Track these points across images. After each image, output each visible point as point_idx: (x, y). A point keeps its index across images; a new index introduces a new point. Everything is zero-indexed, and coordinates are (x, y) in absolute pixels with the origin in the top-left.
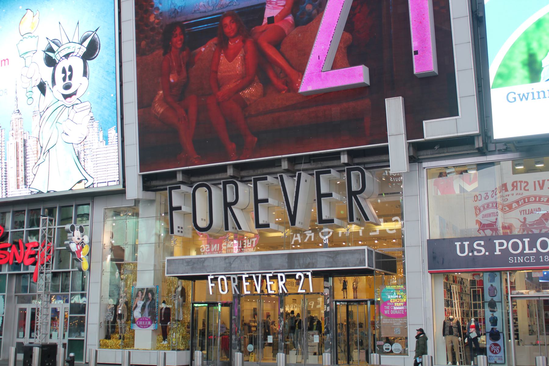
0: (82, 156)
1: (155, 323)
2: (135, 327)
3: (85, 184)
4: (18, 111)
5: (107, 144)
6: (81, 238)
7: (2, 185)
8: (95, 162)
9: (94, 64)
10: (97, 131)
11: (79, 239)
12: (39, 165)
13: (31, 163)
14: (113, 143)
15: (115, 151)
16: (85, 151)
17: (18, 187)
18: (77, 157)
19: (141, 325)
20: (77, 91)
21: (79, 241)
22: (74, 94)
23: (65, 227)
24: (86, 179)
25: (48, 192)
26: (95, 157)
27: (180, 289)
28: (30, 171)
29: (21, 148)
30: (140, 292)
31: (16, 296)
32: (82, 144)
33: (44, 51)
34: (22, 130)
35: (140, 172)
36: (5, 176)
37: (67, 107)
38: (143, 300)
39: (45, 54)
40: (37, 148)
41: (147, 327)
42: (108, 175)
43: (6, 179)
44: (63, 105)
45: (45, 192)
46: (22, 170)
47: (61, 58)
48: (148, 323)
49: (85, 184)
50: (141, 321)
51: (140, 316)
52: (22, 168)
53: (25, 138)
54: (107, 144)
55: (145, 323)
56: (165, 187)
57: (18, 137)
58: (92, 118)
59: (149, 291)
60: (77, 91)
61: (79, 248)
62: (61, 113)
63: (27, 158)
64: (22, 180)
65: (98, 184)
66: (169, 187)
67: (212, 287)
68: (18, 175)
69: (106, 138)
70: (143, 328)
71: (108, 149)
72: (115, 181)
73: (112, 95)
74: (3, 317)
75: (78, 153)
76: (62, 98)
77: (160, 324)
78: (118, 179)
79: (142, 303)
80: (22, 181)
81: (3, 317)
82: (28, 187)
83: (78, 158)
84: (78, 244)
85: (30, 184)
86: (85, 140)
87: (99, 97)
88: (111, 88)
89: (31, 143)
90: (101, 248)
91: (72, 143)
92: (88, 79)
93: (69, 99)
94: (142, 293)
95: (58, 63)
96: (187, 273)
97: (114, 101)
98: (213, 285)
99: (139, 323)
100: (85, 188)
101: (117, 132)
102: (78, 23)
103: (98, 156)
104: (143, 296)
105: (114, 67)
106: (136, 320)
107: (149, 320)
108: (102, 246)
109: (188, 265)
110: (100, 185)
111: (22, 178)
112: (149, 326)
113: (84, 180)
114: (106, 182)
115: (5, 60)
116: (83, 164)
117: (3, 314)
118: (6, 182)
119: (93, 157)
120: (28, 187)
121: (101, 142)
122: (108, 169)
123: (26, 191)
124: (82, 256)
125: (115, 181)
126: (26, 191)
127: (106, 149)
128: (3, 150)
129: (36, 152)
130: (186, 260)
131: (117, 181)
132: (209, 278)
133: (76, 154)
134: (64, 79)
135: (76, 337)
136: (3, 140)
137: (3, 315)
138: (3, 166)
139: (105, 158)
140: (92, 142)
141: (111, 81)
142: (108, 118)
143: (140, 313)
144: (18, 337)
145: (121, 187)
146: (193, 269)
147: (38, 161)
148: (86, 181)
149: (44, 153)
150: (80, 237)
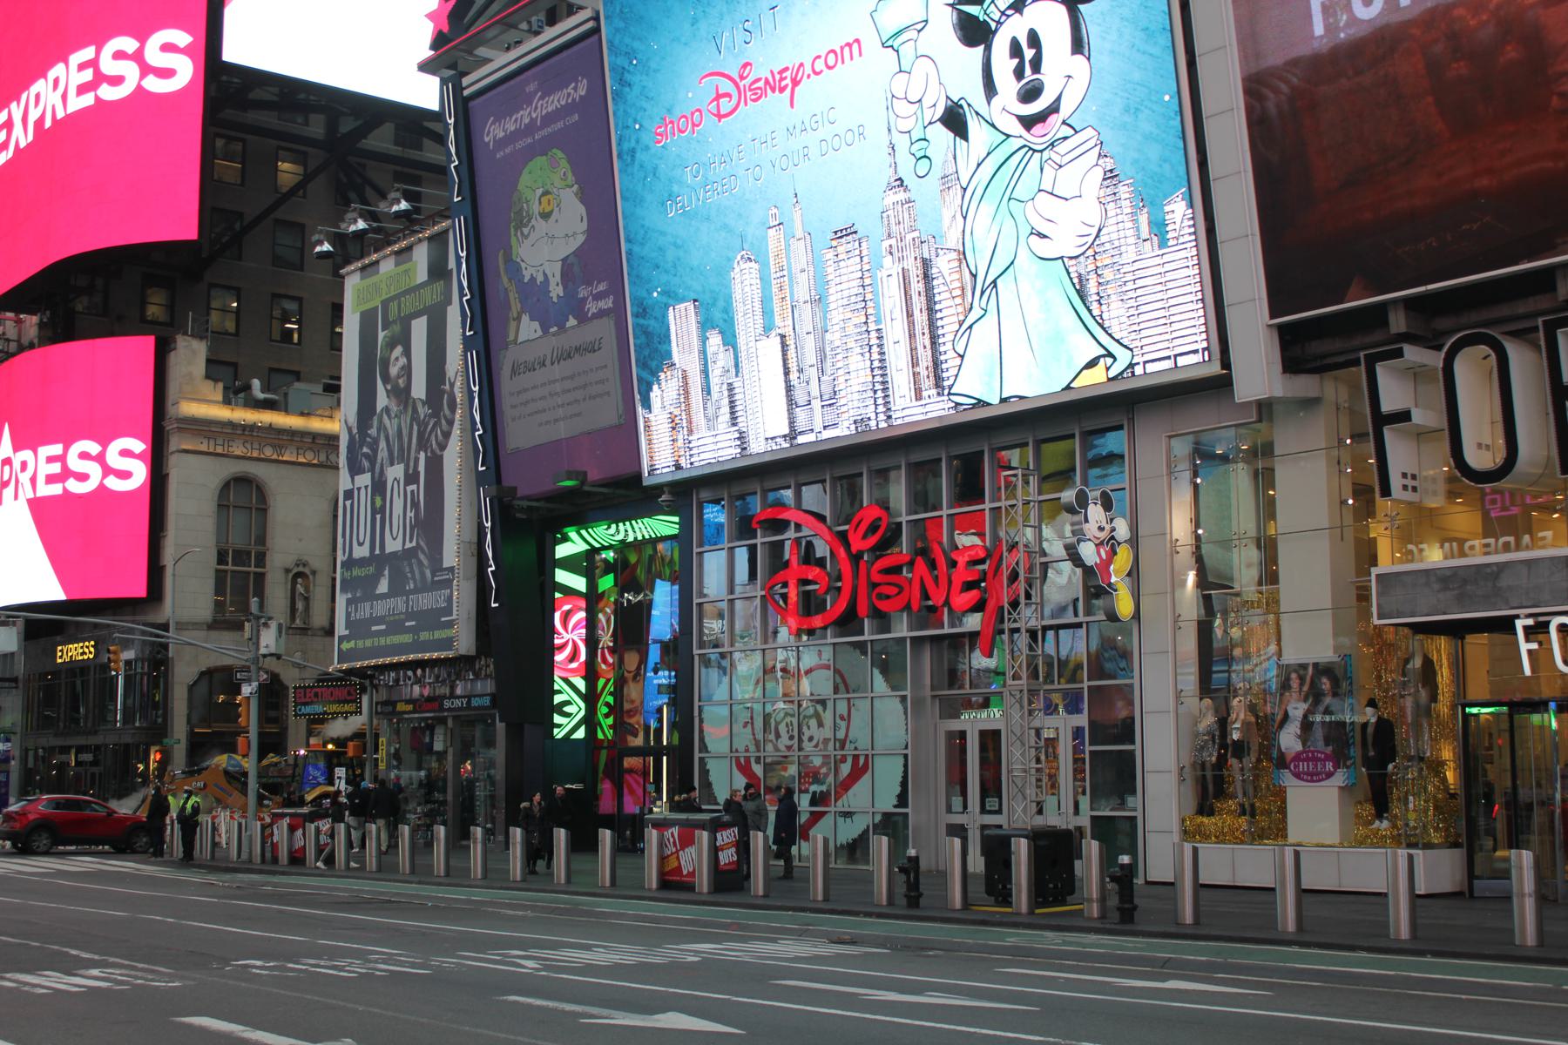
0: (1092, 287)
1: (1348, 767)
2: (1287, 779)
3: (1108, 369)
4: (898, 183)
5: (1163, 244)
6: (1108, 527)
7: (875, 392)
8: (1132, 303)
9: (1102, 14)
10: (1129, 211)
11: (1101, 529)
12: (970, 327)
13: (948, 324)
14: (1180, 241)
15: (1190, 264)
16: (1099, 273)
17: (918, 397)
18: (1078, 291)
19: (1308, 774)
20: (1059, 98)
21: (1102, 535)
22: (1054, 108)
23: (1060, 498)
24: (1110, 355)
25: (1003, 400)
26: (1130, 286)
27: (1417, 662)
28: (949, 346)
29: (917, 286)
30: (1294, 676)
31: (934, 697)
32: (1090, 252)
34: (916, 234)
35: (1272, 316)
36: (881, 368)
37: (1035, 151)
38: (1305, 700)
39: (955, 13)
40: (961, 279)
41: (1320, 780)
42: (1175, 335)
43: (882, 375)
44: (1025, 146)
45: (996, 401)
46: (925, 347)
47: (1003, 13)
48: (1325, 766)
49: (1108, 369)
50: (1303, 760)
51: (1299, 747)
53: (926, 255)
54: (1163, 244)
55: (1316, 765)
56: (1351, 356)
57: (905, 254)
58: (1110, 176)
59: (1322, 670)
60: (1059, 98)
61: (1104, 556)
62: (1021, 169)
63: (936, 312)
65: (1147, 365)
66: (1544, 321)
67: (1530, 652)
69: (1159, 229)
70: (1312, 781)
71: (1167, 258)
72: (1196, 352)
73: (1167, 98)
74: (906, 756)
75: (1080, 281)
76: (1017, 128)
77: (1364, 770)
78: (1205, 344)
79: (1303, 707)
80: (928, 377)
81: (906, 756)
82: (946, 392)
83: (1082, 294)
84: (1102, 543)
86: (1097, 242)
87: (1127, 110)
88: (1162, 76)
89: (944, 265)
90: (1168, 551)
91: (1062, 258)
92: (1089, 59)
93: (1038, 129)
94: (1302, 679)
95: (997, 30)
96: (1445, 614)
97: (1172, 115)
98: (1534, 646)
99: (1295, 767)
100: (1110, 380)
101: (1191, 205)
103: (1140, 283)
104: (1305, 688)
105: (1163, 12)
106: (1288, 758)
107: (1327, 758)
108: (1168, 545)
109: (1445, 589)
110: (1151, 368)
111: (927, 368)
112: (1329, 775)
113: (1104, 356)
114: (1169, 358)
115: (849, 45)
116: (1096, 313)
117: (906, 747)
118: (883, 383)
120: (946, 392)
121: (1145, 241)
122: (1173, 319)
123: (941, 405)
124: (1113, 579)
125: (1196, 352)
126: (941, 405)
128: (869, 297)
129: (958, 292)
130: (1438, 572)
131: (1204, 349)
132: (1519, 624)
133: (1074, 284)
134: (1019, 73)
135: (1111, 810)
136: (866, 267)
137: (905, 752)
138: (874, 341)
139: (1159, 288)
140: (1117, 243)
141: (1158, 58)
142: (1161, 166)
143: (1299, 737)
144: (949, 810)
145: (1215, 369)
146: (1463, 601)
148: (1109, 361)
149: (983, 293)
150: (1104, 524)
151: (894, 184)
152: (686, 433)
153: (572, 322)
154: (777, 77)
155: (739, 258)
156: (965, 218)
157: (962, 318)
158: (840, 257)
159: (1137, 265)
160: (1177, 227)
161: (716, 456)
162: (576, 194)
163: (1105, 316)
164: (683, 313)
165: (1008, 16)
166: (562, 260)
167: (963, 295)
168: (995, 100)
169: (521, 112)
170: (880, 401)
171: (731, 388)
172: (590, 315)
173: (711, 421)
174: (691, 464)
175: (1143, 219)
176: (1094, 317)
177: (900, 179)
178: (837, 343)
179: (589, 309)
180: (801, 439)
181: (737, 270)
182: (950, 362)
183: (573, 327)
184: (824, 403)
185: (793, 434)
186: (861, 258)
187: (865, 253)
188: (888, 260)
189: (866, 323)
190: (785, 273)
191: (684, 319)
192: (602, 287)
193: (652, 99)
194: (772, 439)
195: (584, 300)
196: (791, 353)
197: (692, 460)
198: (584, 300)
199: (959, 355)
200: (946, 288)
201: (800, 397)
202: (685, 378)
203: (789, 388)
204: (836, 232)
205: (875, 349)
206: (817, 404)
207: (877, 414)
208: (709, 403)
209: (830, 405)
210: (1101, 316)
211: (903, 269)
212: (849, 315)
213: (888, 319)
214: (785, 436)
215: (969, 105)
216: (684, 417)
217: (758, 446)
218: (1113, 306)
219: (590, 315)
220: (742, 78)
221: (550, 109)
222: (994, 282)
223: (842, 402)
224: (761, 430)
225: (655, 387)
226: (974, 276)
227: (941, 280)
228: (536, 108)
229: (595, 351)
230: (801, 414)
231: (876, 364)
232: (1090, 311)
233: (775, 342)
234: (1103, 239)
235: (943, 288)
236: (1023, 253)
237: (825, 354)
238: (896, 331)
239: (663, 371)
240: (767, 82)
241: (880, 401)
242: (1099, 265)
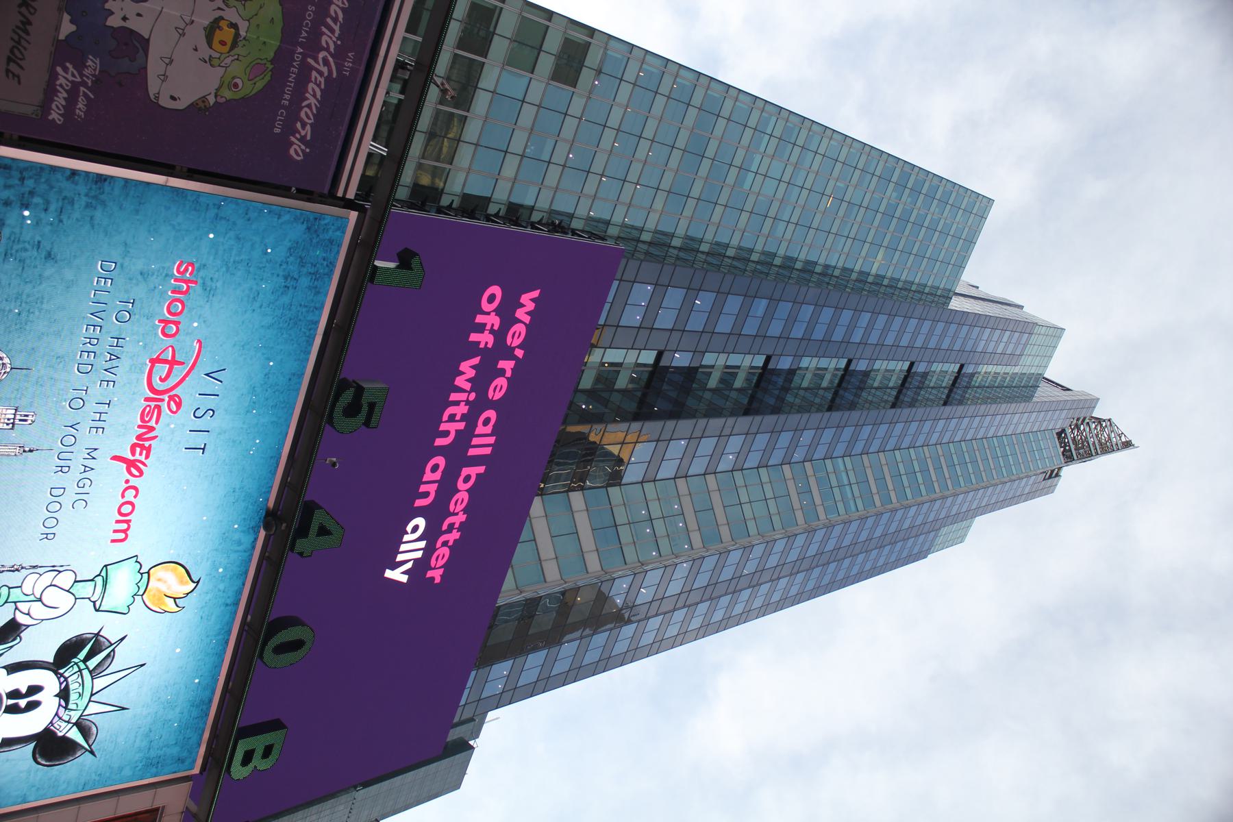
33: (98, 634)
102: (123, 709)
153: (67, 28)
162: (204, 99)
165: (61, 684)
166: (148, 41)
169: (337, 32)
172: (59, 69)
179: (66, 70)
183: (58, 29)
192: (81, 105)
195: (80, 66)
198: (80, 66)
215: (11, 647)
219: (59, 69)
220: (171, 398)
221: (311, 86)
228: (326, 62)
229: (9, 60)
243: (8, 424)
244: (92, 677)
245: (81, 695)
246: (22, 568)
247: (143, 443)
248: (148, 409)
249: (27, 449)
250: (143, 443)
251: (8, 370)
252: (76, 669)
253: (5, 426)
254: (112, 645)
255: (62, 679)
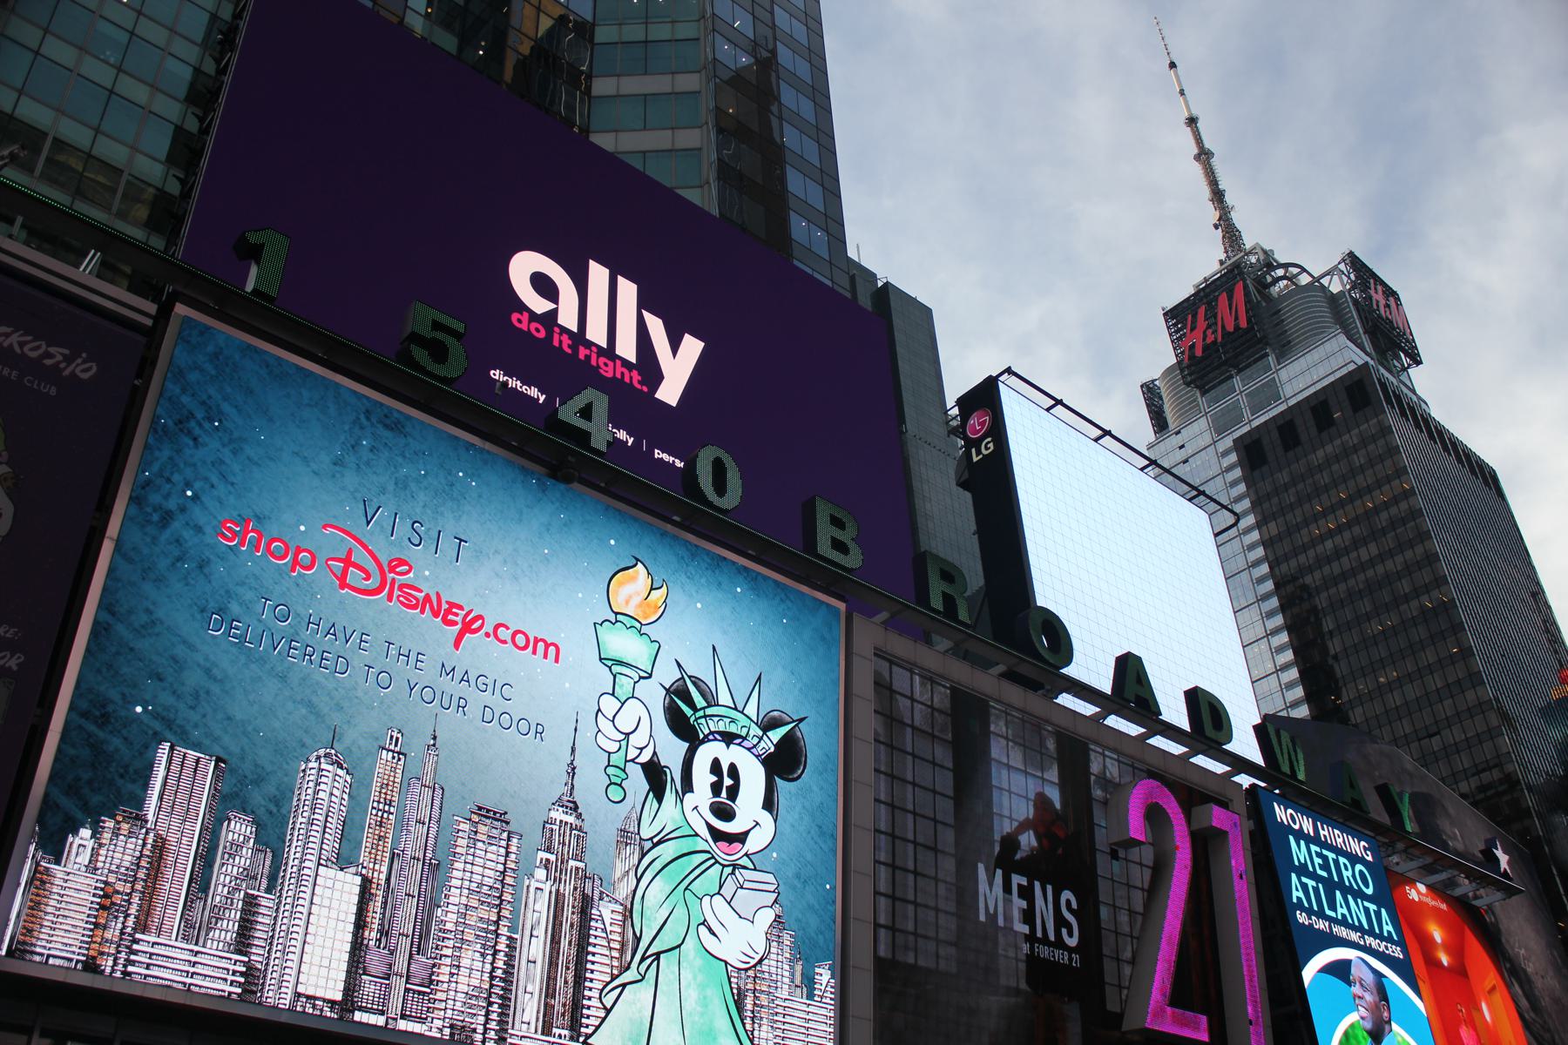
0: (749, 1001)
4: (571, 805)
5: (810, 996)
7: (490, 1004)
8: (779, 1033)
10: (788, 955)
12: (624, 986)
13: (600, 969)
14: (824, 1000)
22: (741, 838)
28: (595, 994)
29: (570, 916)
32: (751, 973)
33: (667, 690)
34: (581, 865)
36: (503, 980)
37: (717, 862)
44: (708, 852)
46: (566, 982)
52: (565, 976)
53: (588, 891)
54: (810, 996)
60: (747, 833)
64: (561, 1010)
68: (550, 991)
69: (809, 983)
71: (811, 1009)
75: (739, 994)
76: (705, 833)
80: (563, 1015)
82: (581, 1039)
85: (590, 1030)
87: (798, 876)
89: (606, 912)
91: (726, 963)
92: (775, 821)
102: (759, 678)
103: (788, 1019)
115: (547, 646)
116: (748, 1027)
119: (775, 1018)
127: (804, 1007)
128: (507, 897)
129: (617, 946)
133: (733, 994)
139: (803, 1030)
147: (621, 974)
149: (643, 959)
151: (568, 804)
152: (131, 922)
154: (445, 606)
155: (322, 752)
156: (639, 881)
157: (615, 972)
158: (479, 837)
159: (787, 1004)
160: (823, 988)
161: (189, 980)
163: (756, 1033)
164: (190, 763)
165: (716, 739)
167: (622, 951)
168: (688, 795)
170: (494, 1016)
171: (251, 903)
173: (193, 931)
174: (125, 973)
175: (799, 968)
176: (746, 1031)
177: (574, 803)
178: (449, 926)
180: (358, 1016)
181: (313, 764)
182: (593, 1012)
184: (408, 986)
185: (348, 1002)
186: (508, 853)
187: (513, 849)
188: (541, 873)
189: (497, 923)
190: (392, 810)
191: (188, 771)
193: (232, 484)
194: (309, 997)
196: (376, 905)
197: (130, 969)
199: (605, 1008)
200: (604, 935)
201: (374, 960)
202: (161, 846)
203: (358, 947)
204: (480, 808)
205: (501, 955)
206: (399, 984)
207: (486, 1029)
208: (199, 905)
209: (420, 993)
210: (752, 1032)
211: (558, 891)
212: (475, 903)
213: (527, 933)
214: (332, 1003)
216: (136, 900)
217: (278, 996)
218: (764, 1028)
220: (392, 570)
222: (658, 955)
223: (440, 995)
224: (292, 980)
225: (85, 833)
226: (638, 939)
227: (599, 925)
230: (369, 988)
231: (499, 973)
232: (744, 1024)
233: (348, 884)
234: (765, 968)
235: (599, 933)
236: (690, 944)
237: (429, 932)
238: (536, 948)
239: (113, 817)
240: (427, 598)
241: (494, 1016)
242: (758, 988)
243: (399, 759)
244: (715, 705)
245: (733, 721)
246: (572, 764)
247: (445, 611)
248: (401, 599)
249: (432, 742)
250: (445, 611)
251: (333, 752)
252: (703, 721)
253: (402, 762)
254: (683, 678)
255: (711, 737)
